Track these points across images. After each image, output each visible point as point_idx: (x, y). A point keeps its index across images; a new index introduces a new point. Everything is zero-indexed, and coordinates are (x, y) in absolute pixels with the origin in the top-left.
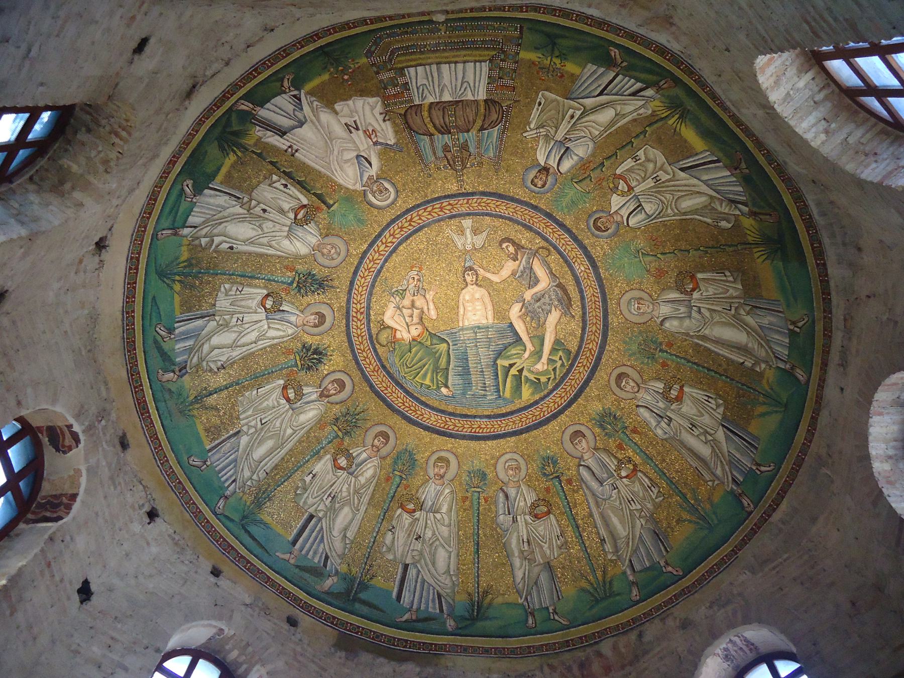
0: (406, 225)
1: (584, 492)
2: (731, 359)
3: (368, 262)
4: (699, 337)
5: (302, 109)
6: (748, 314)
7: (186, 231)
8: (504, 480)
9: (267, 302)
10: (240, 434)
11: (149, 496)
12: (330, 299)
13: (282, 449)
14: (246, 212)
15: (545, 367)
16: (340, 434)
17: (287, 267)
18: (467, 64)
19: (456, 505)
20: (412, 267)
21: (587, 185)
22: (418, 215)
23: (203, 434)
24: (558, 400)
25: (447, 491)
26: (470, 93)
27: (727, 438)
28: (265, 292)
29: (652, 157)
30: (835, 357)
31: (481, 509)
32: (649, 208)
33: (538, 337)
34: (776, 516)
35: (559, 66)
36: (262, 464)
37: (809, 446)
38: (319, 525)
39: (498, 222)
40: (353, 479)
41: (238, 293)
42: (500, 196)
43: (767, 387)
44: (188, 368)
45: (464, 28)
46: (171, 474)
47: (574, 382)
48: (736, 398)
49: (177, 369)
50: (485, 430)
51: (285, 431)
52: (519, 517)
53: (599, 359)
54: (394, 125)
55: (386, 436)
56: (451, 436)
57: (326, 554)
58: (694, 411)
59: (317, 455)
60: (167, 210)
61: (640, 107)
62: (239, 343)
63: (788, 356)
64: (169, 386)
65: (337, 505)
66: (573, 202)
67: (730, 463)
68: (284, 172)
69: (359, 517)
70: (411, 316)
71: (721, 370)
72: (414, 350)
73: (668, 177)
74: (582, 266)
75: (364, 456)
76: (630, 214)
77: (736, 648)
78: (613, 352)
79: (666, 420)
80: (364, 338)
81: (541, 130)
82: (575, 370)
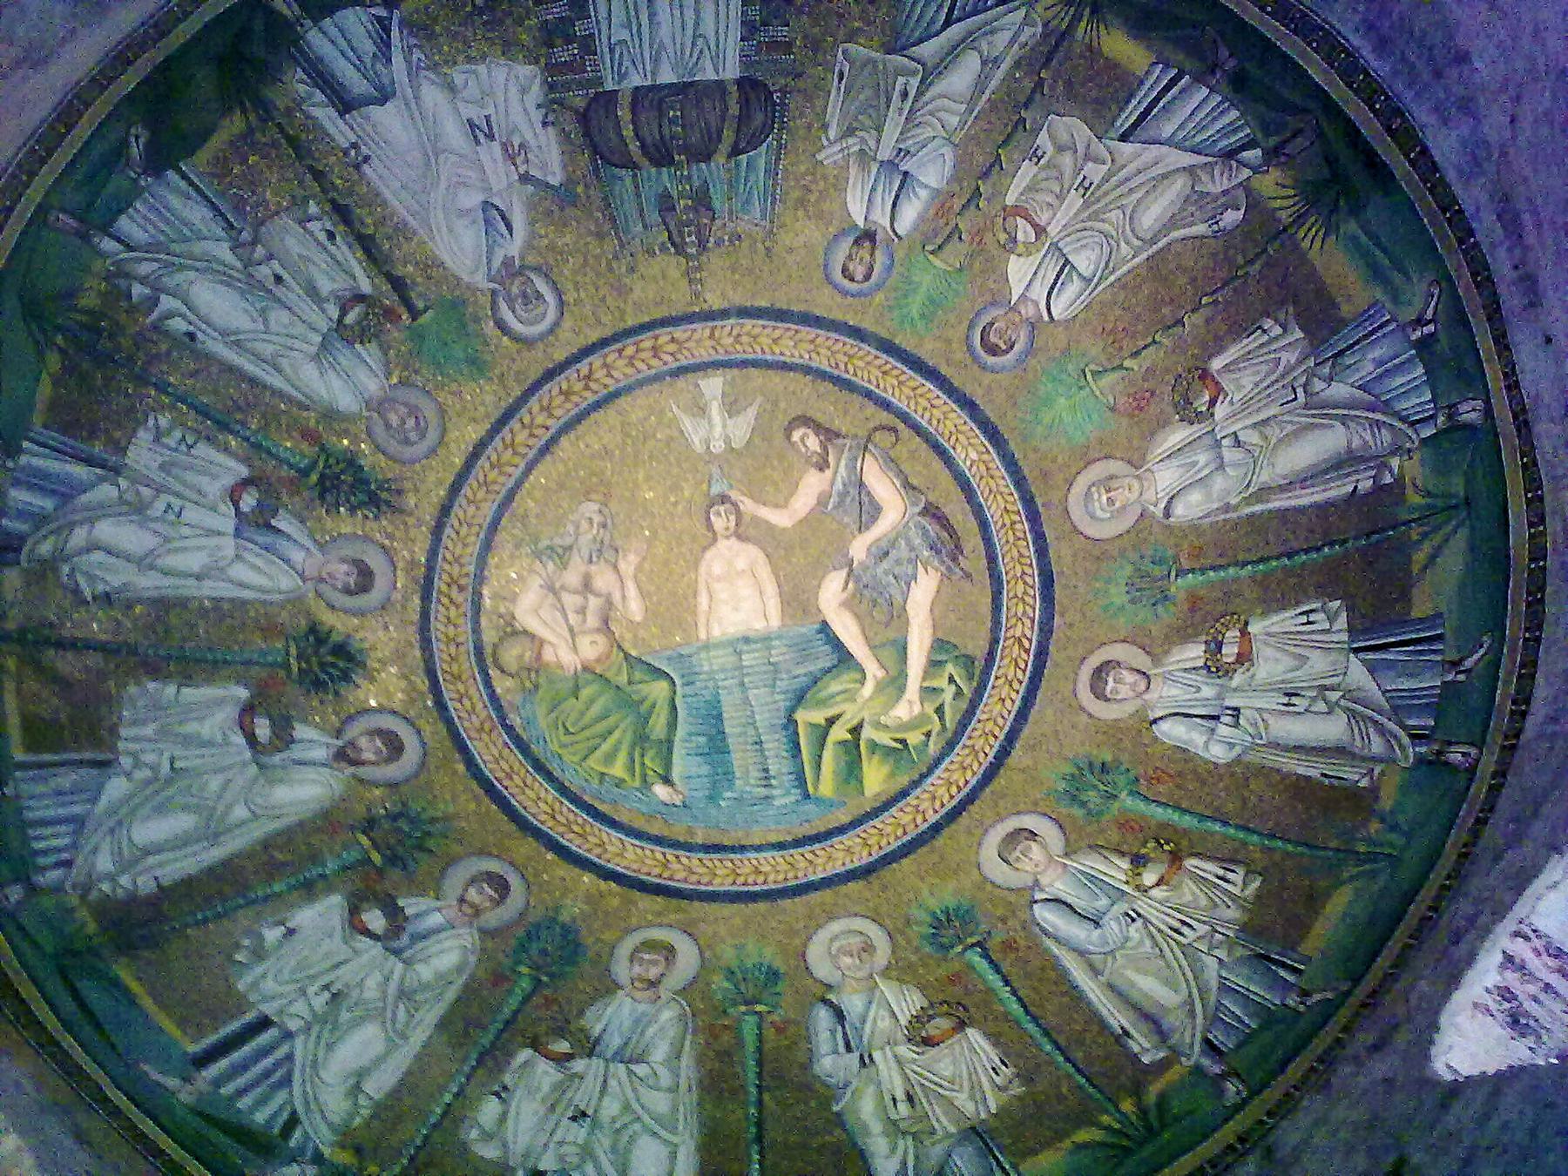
0: (578, 386)
4: (1247, 501)
6: (1330, 379)
7: (108, 245)
9: (245, 496)
12: (390, 537)
14: (239, 265)
15: (917, 709)
16: (376, 858)
21: (956, 253)
22: (605, 365)
23: (14, 721)
24: (955, 776)
25: (667, 1015)
27: (1372, 669)
28: (244, 471)
29: (1064, 137)
30: (1511, 299)
32: (1084, 262)
33: (894, 642)
34: (1531, 725)
36: (151, 860)
39: (776, 379)
41: (183, 448)
42: (781, 315)
44: (23, 557)
47: (990, 725)
51: (230, 807)
52: (877, 1055)
53: (1042, 654)
54: (565, 136)
55: (502, 886)
57: (294, 1113)
59: (309, 890)
65: (345, 1016)
66: (932, 301)
67: (1397, 711)
68: (333, 201)
70: (582, 611)
72: (586, 693)
73: (1106, 168)
74: (971, 452)
75: (436, 919)
76: (1049, 294)
77: (1532, 989)
80: (462, 649)
81: (851, 141)
82: (990, 696)
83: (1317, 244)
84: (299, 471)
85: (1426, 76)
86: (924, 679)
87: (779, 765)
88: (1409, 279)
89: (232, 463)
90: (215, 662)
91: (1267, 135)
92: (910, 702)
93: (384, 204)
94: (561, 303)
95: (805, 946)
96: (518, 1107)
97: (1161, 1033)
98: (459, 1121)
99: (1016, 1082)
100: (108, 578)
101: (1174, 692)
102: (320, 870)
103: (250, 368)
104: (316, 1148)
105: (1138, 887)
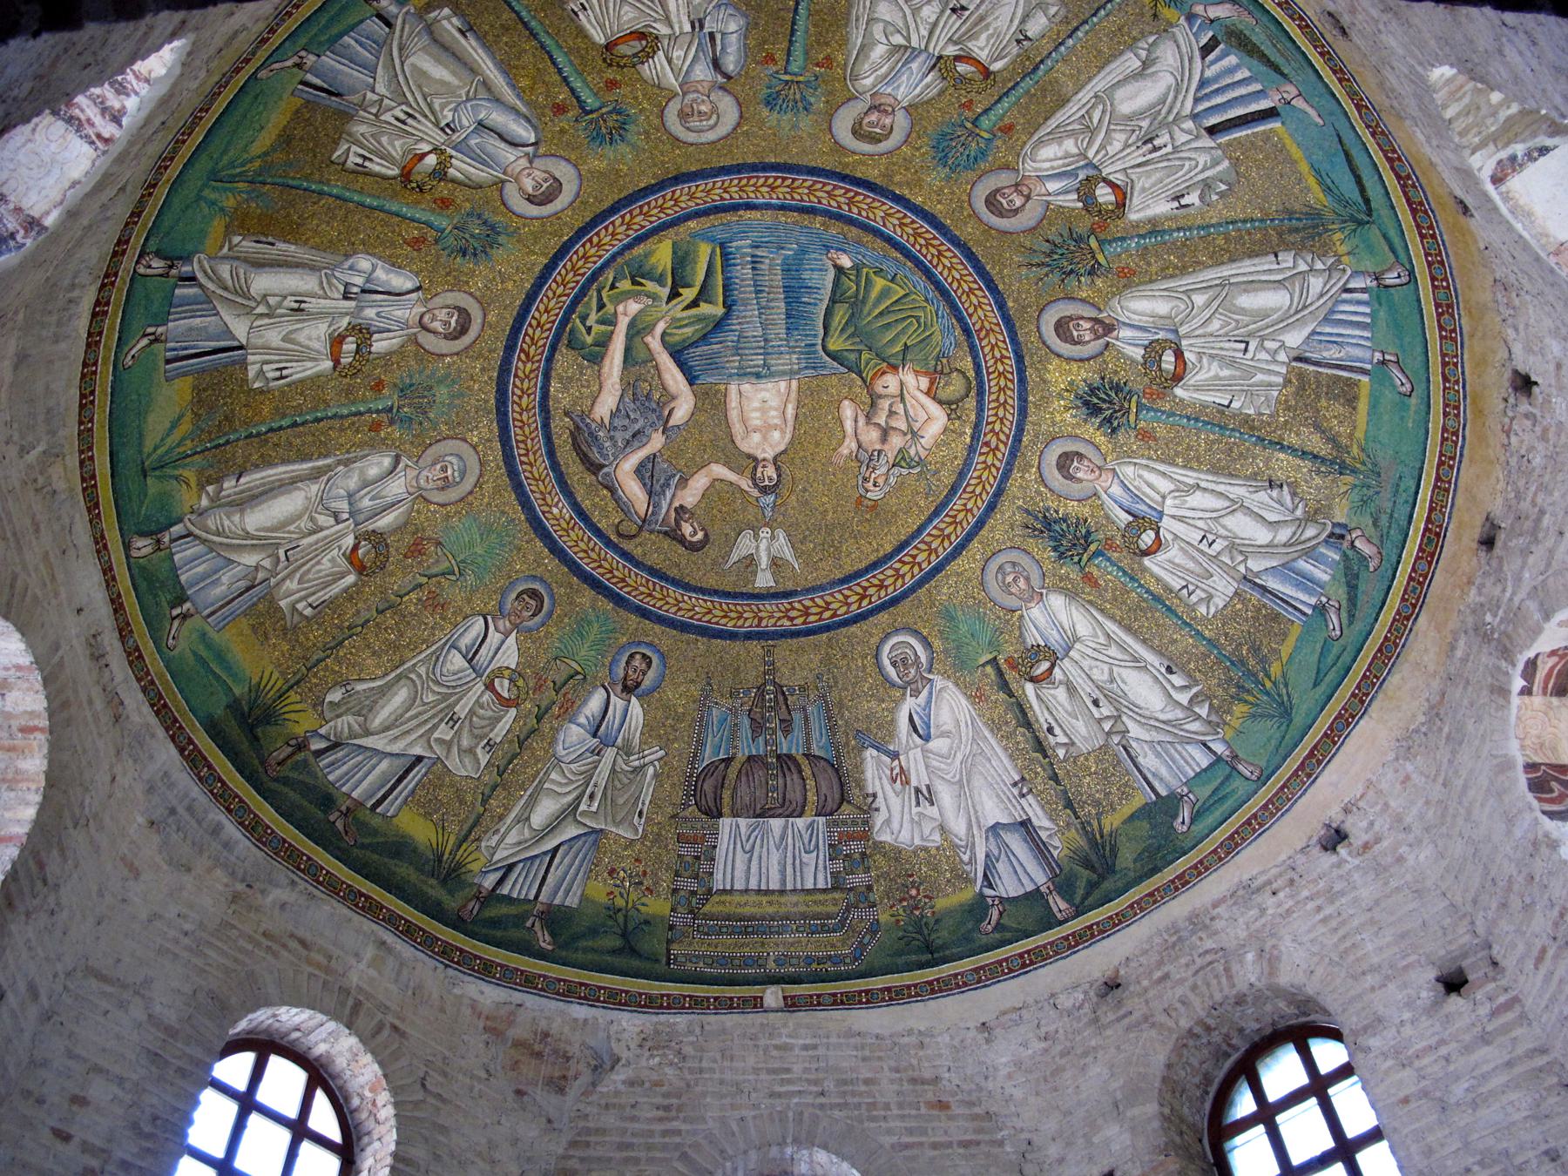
0: (872, 591)
2: (262, 470)
3: (953, 538)
5: (987, 856)
6: (257, 568)
7: (1219, 748)
10: (1294, 354)
11: (1510, 414)
12: (1039, 493)
14: (1124, 718)
15: (620, 308)
16: (1093, 243)
17: (1096, 584)
18: (742, 887)
19: (848, 56)
20: (874, 507)
22: (849, 605)
23: (1363, 406)
24: (593, 251)
25: (868, 82)
26: (743, 830)
27: (228, 333)
28: (1147, 561)
29: (466, 760)
30: (110, 641)
31: (785, 45)
32: (457, 661)
35: (617, 891)
37: (81, 452)
38: (1200, 108)
39: (711, 582)
40: (1091, 154)
41: (1191, 588)
42: (704, 632)
43: (186, 473)
45: (746, 962)
46: (1452, 409)
47: (559, 291)
48: (233, 411)
49: (1346, 544)
50: (761, 181)
52: (687, 28)
53: (510, 348)
54: (860, 784)
55: (991, 202)
56: (844, 178)
57: (1203, 58)
58: (301, 338)
59: (1154, 228)
60: (1229, 803)
61: (498, 844)
62: (1227, 504)
63: (172, 554)
64: (1370, 531)
65: (1145, 124)
68: (1045, 756)
69: (1100, 83)
70: (891, 413)
71: (274, 438)
72: (899, 348)
73: (436, 735)
74: (558, 511)
75: (1053, 186)
78: (483, 369)
79: (355, 290)
80: (993, 397)
81: (636, 763)
83: (267, 675)
84: (1103, 555)
85: (181, 810)
86: (612, 332)
87: (743, 272)
88: (195, 654)
89: (1156, 569)
90: (1197, 420)
91: (305, 761)
92: (625, 314)
93: (1006, 749)
94: (877, 656)
95: (739, 125)
98: (1066, 20)
100: (1267, 500)
101: (399, 313)
103: (1129, 640)
104: (1191, 26)
105: (443, 152)
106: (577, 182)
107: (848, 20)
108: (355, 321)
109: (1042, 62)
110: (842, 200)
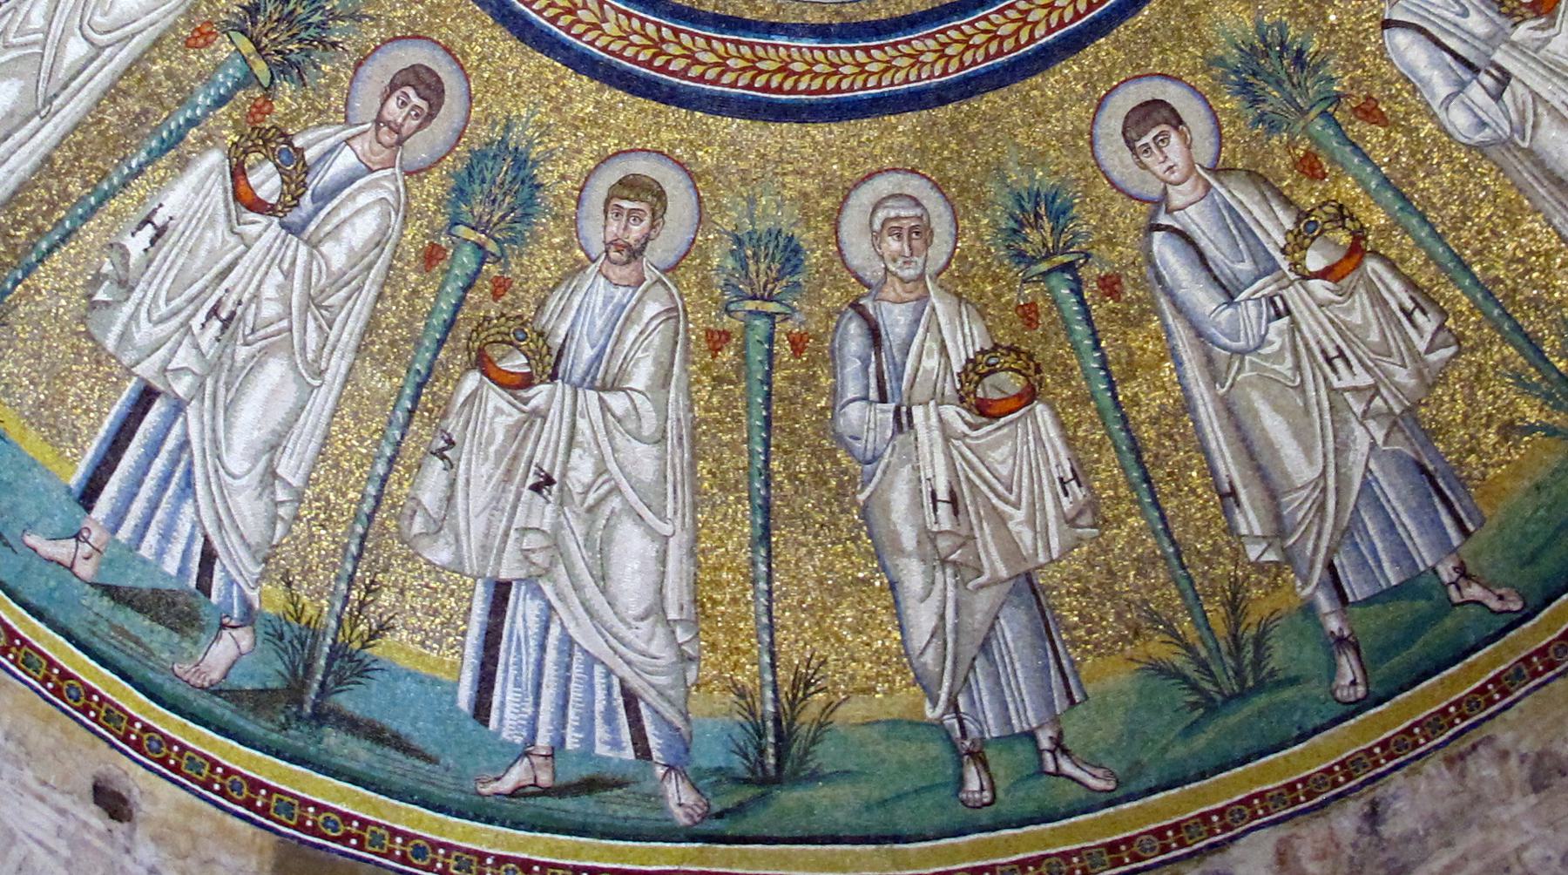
1: (1165, 325)
8: (868, 275)
13: (45, 119)
19: (686, 361)
25: (652, 309)
31: (778, 376)
40: (303, 250)
50: (807, 78)
52: (918, 412)
55: (428, 86)
56: (673, 97)
65: (242, 353)
69: (323, 401)
79: (1487, 80)
96: (468, 470)
97: (1279, 529)
99: (1086, 519)
102: (189, 114)
106: (1098, 131)
107: (694, 441)
108: (1506, 23)
109: (411, 412)
110: (673, 49)
